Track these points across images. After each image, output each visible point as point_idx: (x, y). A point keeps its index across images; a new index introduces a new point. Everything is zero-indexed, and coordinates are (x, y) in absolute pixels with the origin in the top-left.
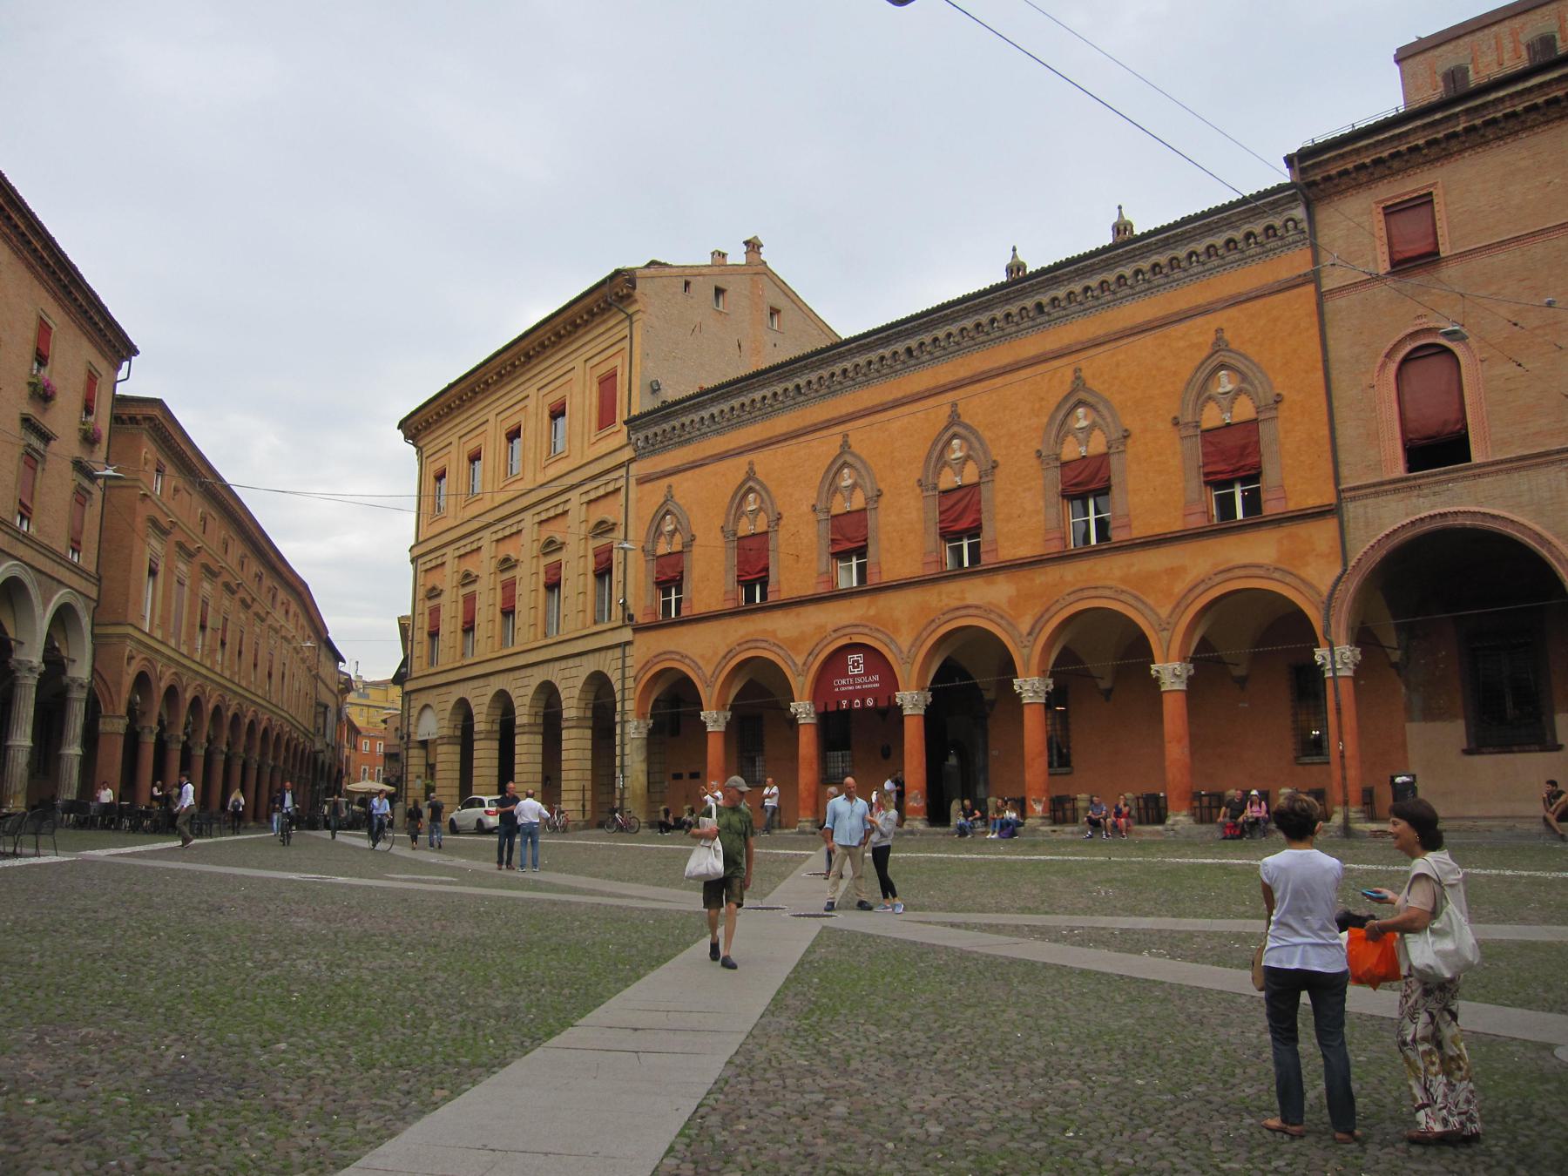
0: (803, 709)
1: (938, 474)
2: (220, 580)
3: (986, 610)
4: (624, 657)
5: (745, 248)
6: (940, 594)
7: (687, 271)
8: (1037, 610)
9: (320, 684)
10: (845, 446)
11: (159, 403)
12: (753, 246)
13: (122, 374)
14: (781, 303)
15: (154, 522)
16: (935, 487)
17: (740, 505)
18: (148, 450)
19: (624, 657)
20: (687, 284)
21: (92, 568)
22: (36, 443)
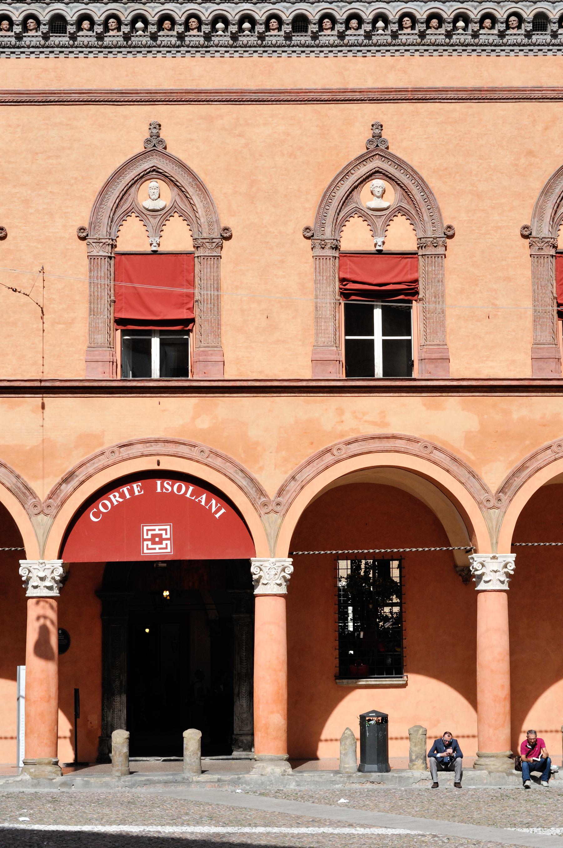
0: (41, 569)
1: (339, 225)
3: (431, 448)
6: (340, 411)
8: (516, 458)
10: (155, 144)
16: (336, 248)
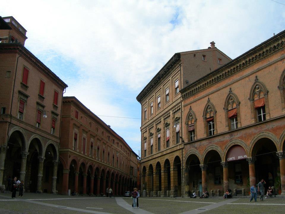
2: (96, 138)
4: (182, 152)
5: (210, 45)
7: (194, 52)
9: (131, 162)
11: (74, 98)
12: (213, 44)
13: (64, 92)
14: (222, 57)
15: (75, 125)
17: (207, 110)
18: (73, 108)
19: (182, 152)
20: (195, 55)
21: (58, 136)
22: (40, 108)
